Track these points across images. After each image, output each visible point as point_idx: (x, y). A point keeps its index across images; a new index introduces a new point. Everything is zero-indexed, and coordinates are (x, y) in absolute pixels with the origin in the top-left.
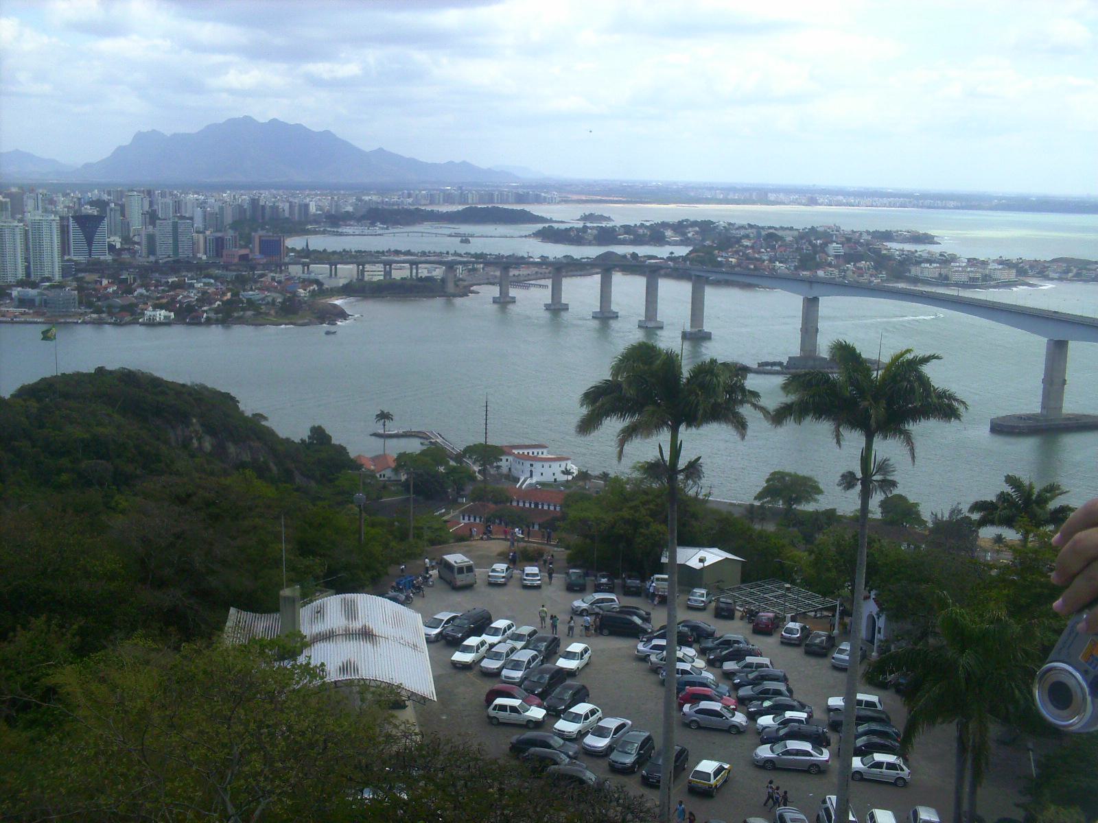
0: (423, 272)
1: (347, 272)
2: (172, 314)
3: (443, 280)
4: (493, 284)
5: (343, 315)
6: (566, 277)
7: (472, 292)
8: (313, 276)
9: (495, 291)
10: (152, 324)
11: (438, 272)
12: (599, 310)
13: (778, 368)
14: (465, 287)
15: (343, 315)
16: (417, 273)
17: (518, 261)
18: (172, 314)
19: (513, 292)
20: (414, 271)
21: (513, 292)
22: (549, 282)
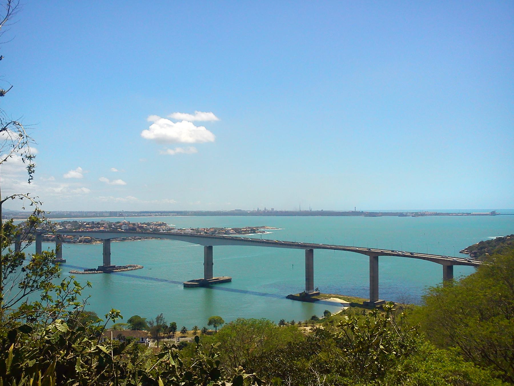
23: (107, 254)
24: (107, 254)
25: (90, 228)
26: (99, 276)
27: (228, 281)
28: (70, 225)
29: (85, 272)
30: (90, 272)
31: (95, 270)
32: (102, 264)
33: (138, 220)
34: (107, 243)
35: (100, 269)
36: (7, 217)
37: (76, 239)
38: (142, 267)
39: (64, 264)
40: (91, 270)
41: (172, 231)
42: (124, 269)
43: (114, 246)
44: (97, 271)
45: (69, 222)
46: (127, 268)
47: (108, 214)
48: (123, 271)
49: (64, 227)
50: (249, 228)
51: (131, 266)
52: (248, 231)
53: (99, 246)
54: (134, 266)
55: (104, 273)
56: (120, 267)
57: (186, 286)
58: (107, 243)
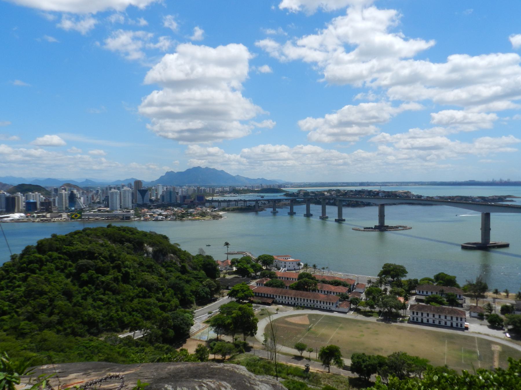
0: (248, 204)
1: (224, 205)
2: (164, 217)
3: (254, 206)
4: (271, 208)
5: (221, 217)
6: (295, 205)
7: (264, 210)
8: (213, 206)
9: (272, 209)
10: (157, 220)
11: (253, 203)
12: (306, 213)
13: (371, 230)
14: (262, 209)
15: (221, 217)
16: (246, 205)
17: (279, 200)
18: (164, 217)
19: (277, 210)
20: (237, 203)
21: (277, 210)
22: (289, 207)
23: (382, 216)
24: (382, 216)
25: (354, 195)
26: (376, 233)
27: (506, 246)
28: (334, 192)
29: (365, 230)
30: (370, 230)
31: (372, 228)
32: (377, 223)
33: (401, 190)
34: (382, 208)
35: (376, 228)
36: (287, 186)
37: (345, 203)
38: (410, 228)
39: (343, 222)
40: (369, 228)
41: (423, 198)
42: (396, 229)
43: (388, 210)
44: (374, 229)
45: (333, 190)
46: (398, 228)
47: (358, 184)
48: (396, 230)
49: (330, 193)
50: (496, 196)
51: (401, 227)
52: (495, 199)
53: (374, 211)
54: (404, 227)
55: (380, 231)
56: (392, 227)
57: (465, 248)
58: (382, 208)
